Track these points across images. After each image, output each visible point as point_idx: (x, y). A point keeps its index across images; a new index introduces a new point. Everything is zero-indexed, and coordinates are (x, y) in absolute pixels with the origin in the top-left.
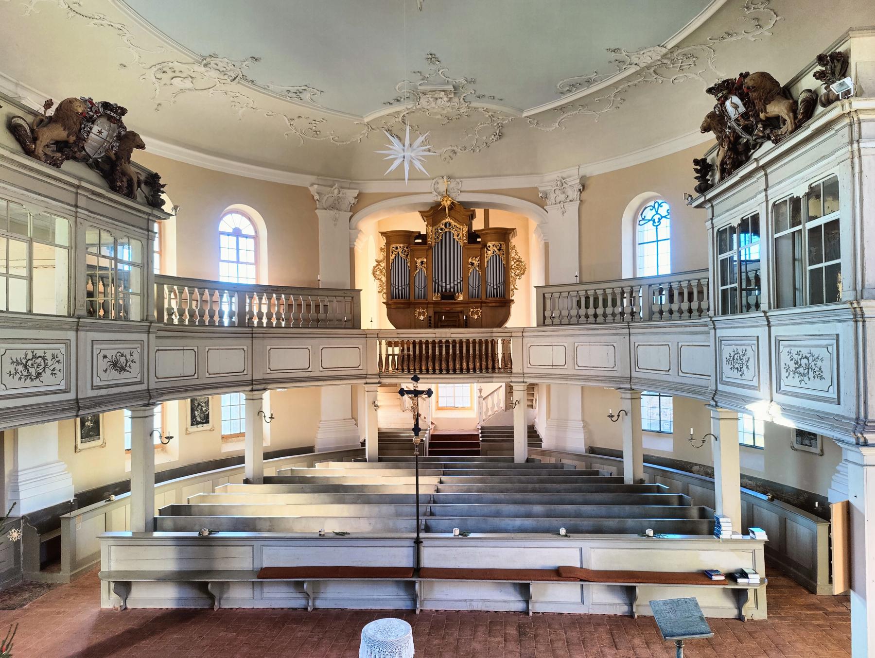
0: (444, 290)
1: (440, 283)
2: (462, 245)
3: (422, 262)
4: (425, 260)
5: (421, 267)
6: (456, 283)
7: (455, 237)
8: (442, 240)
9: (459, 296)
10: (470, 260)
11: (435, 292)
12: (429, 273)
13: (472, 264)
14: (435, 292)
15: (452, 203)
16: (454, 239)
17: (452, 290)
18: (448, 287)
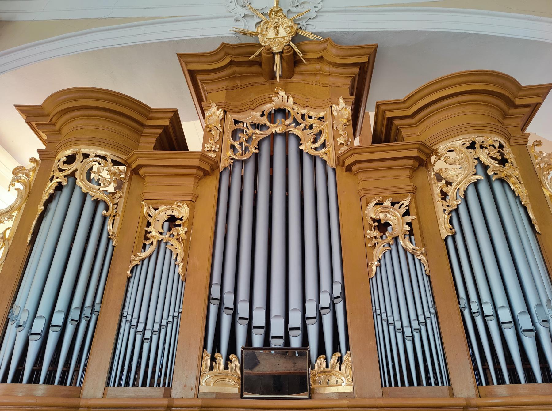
0: (257, 341)
1: (243, 310)
2: (331, 163)
3: (172, 220)
4: (183, 211)
5: (166, 237)
6: (311, 310)
7: (307, 146)
8: (257, 157)
9: (327, 372)
10: (372, 212)
11: (217, 347)
12: (195, 261)
13: (383, 227)
14: (217, 347)
15: (296, 38)
16: (301, 152)
17: (296, 342)
18: (277, 328)
